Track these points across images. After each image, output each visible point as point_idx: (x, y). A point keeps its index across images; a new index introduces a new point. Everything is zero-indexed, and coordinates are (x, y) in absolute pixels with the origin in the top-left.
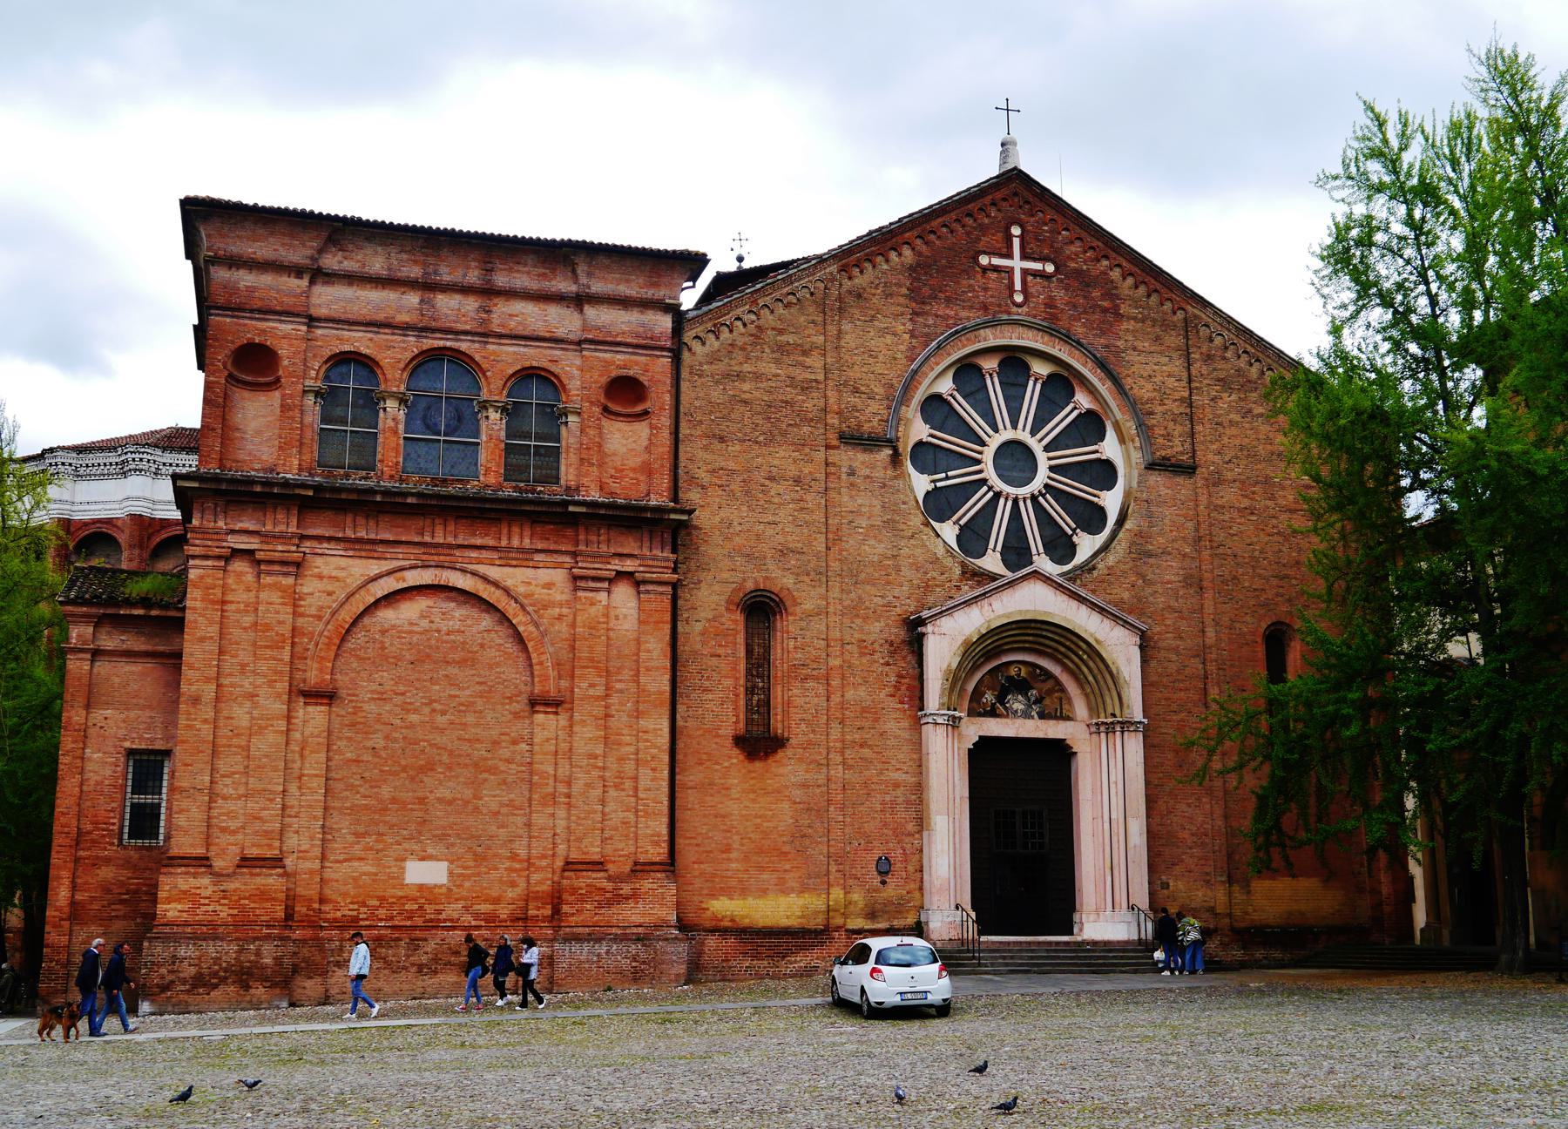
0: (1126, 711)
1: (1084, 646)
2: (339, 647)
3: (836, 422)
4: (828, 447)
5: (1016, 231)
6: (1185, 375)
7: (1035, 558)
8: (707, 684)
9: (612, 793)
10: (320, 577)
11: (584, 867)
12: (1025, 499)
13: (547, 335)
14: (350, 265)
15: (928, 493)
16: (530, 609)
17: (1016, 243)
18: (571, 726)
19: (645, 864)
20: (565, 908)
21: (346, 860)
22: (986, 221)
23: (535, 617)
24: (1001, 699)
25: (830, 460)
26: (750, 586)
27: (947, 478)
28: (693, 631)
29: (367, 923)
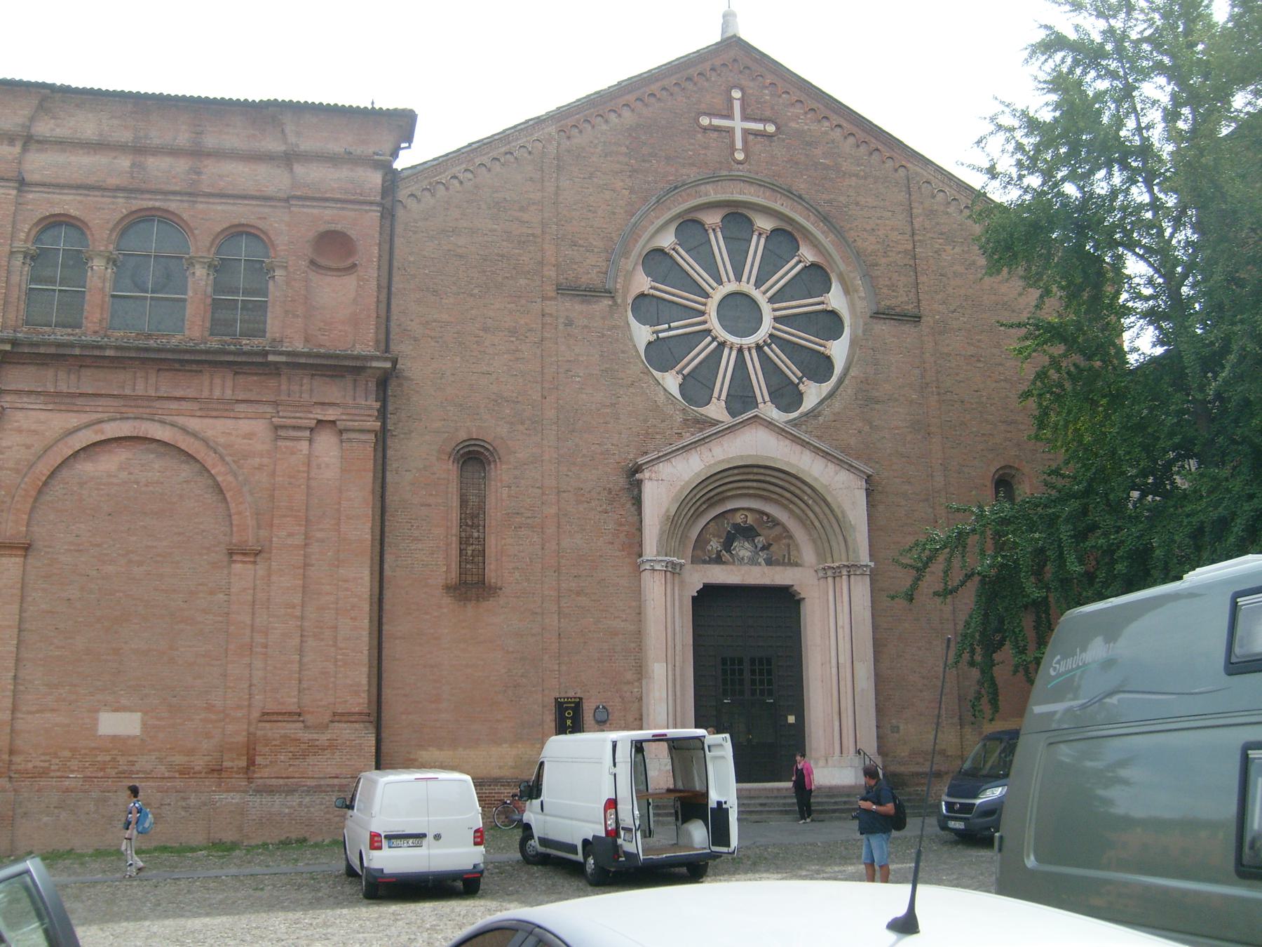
0: (851, 557)
1: (809, 491)
2: (36, 500)
3: (553, 274)
4: (544, 298)
5: (736, 94)
6: (907, 230)
7: (761, 406)
8: (416, 533)
9: (311, 642)
10: (20, 431)
11: (280, 718)
12: (749, 349)
13: (257, 194)
14: (60, 132)
15: (650, 343)
16: (228, 459)
17: (737, 106)
18: (269, 576)
19: (342, 714)
20: (259, 760)
21: (38, 712)
22: (706, 84)
23: (234, 467)
24: (728, 545)
25: (547, 310)
26: (463, 435)
27: (670, 329)
28: (402, 481)
29: (59, 774)
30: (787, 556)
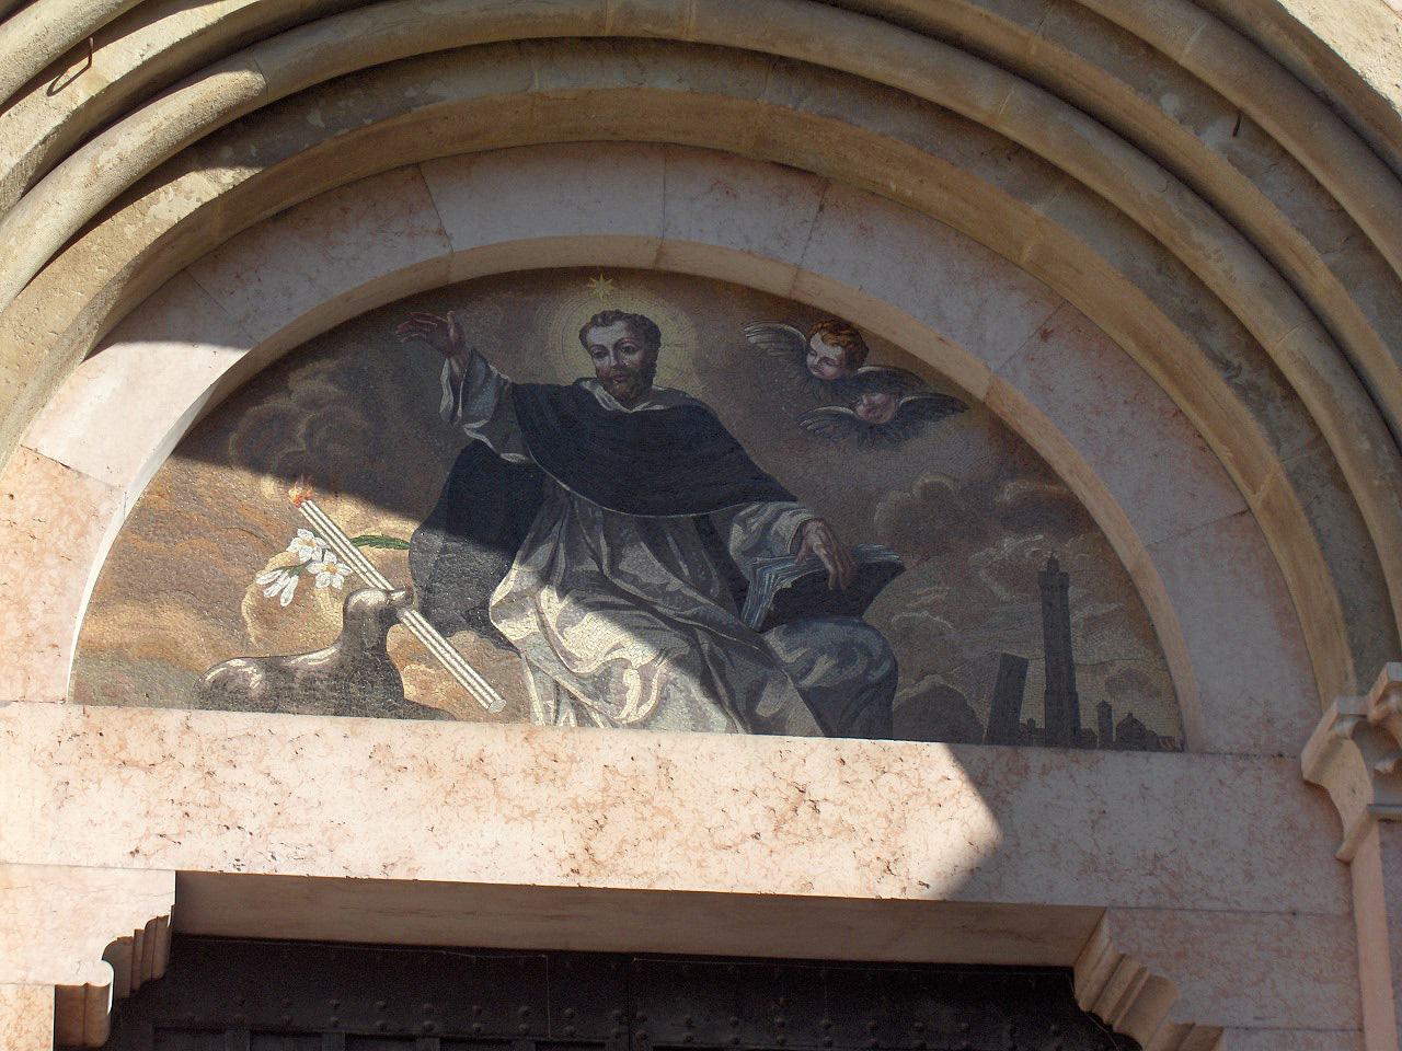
30: (1036, 674)
